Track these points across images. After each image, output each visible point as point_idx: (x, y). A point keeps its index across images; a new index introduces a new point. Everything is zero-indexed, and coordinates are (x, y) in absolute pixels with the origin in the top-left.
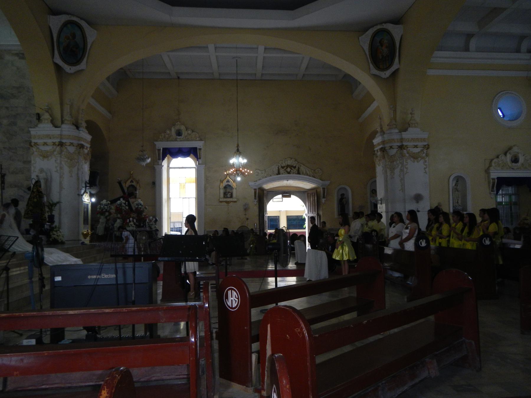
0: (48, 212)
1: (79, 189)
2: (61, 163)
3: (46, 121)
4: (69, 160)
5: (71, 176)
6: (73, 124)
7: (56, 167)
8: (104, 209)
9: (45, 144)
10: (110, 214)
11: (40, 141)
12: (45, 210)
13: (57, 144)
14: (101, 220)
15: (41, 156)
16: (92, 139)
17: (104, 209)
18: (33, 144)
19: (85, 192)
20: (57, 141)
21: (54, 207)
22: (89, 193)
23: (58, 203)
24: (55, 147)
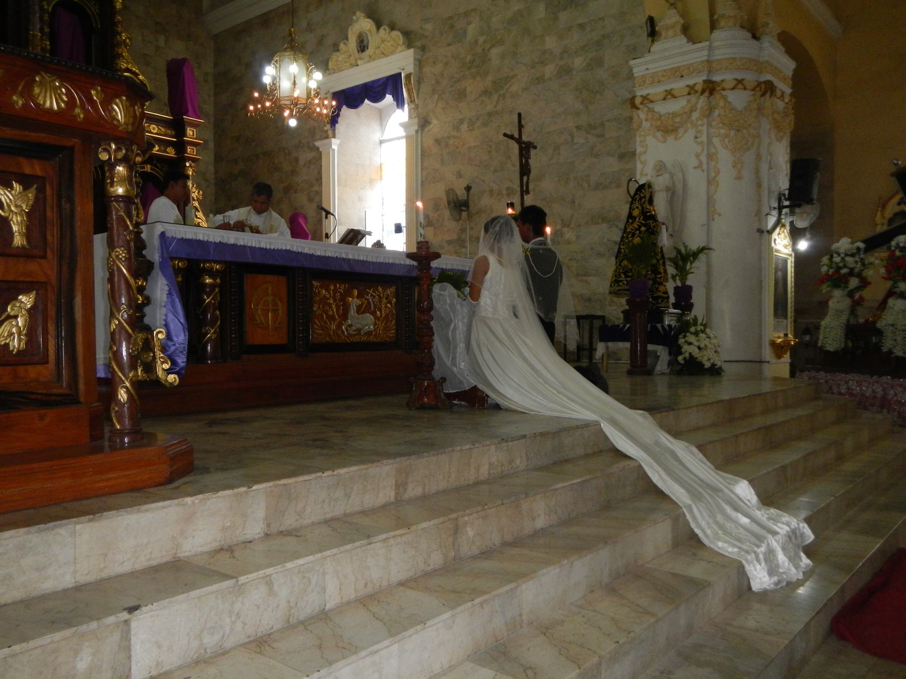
0: (674, 277)
1: (760, 215)
2: (710, 142)
3: (671, 33)
4: (733, 133)
5: (739, 178)
6: (742, 27)
7: (697, 156)
8: (845, 266)
9: (670, 95)
10: (865, 283)
11: (656, 91)
12: (665, 271)
13: (699, 88)
14: (832, 304)
15: (658, 129)
16: (796, 71)
17: (845, 266)
18: (638, 101)
19: (778, 223)
20: (698, 80)
21: (691, 263)
22: (788, 227)
23: (702, 250)
24: (693, 98)
